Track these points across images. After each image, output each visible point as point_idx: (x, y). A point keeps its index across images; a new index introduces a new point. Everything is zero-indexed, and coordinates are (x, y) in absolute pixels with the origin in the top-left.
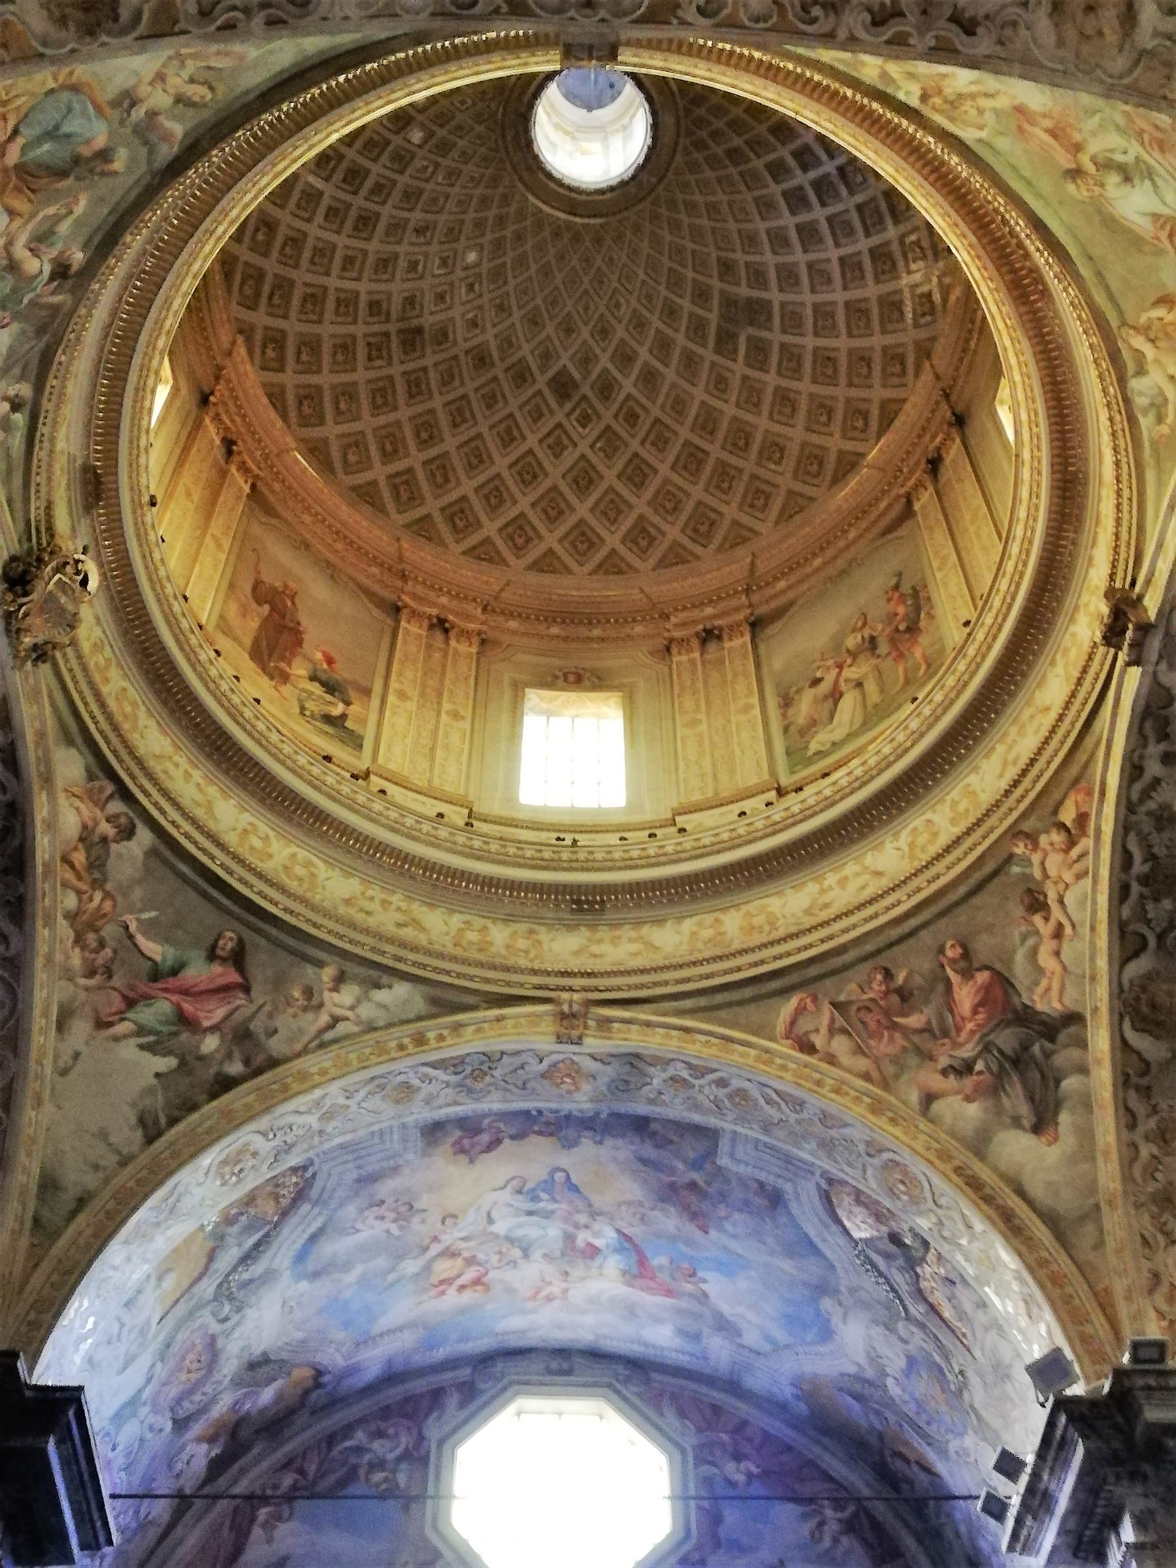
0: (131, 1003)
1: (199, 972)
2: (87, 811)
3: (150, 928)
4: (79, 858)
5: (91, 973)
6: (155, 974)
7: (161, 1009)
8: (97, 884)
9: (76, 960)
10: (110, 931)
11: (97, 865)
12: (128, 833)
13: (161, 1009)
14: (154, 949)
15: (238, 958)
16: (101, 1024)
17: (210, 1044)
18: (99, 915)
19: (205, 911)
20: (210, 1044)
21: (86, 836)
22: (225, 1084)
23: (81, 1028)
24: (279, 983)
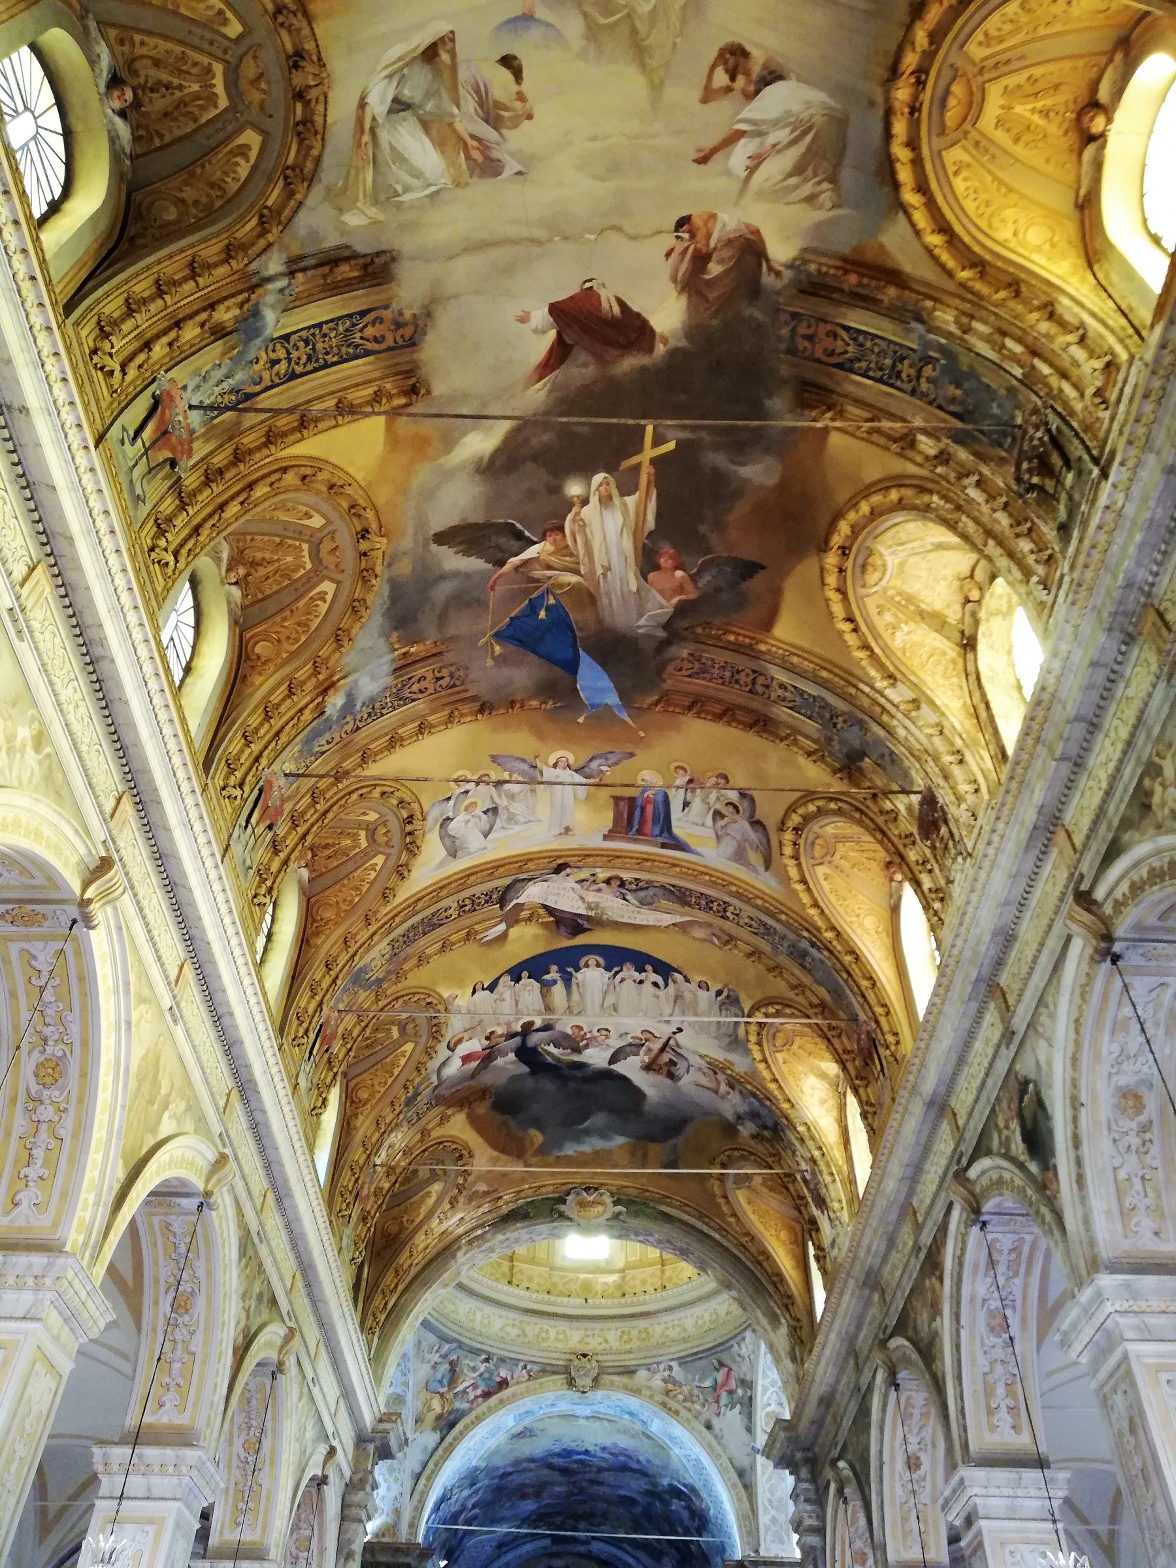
0: (717, 1402)
1: (720, 1376)
2: (658, 1377)
3: (701, 1380)
4: (670, 1387)
5: (703, 1405)
6: (714, 1388)
7: (724, 1395)
8: (681, 1386)
9: (697, 1407)
10: (696, 1392)
11: (675, 1382)
12: (670, 1368)
13: (724, 1395)
14: (708, 1383)
15: (721, 1364)
16: (718, 1414)
17: (740, 1392)
18: (690, 1391)
19: (705, 1362)
20: (740, 1392)
21: (665, 1381)
22: (750, 1398)
23: (715, 1422)
24: (734, 1361)
